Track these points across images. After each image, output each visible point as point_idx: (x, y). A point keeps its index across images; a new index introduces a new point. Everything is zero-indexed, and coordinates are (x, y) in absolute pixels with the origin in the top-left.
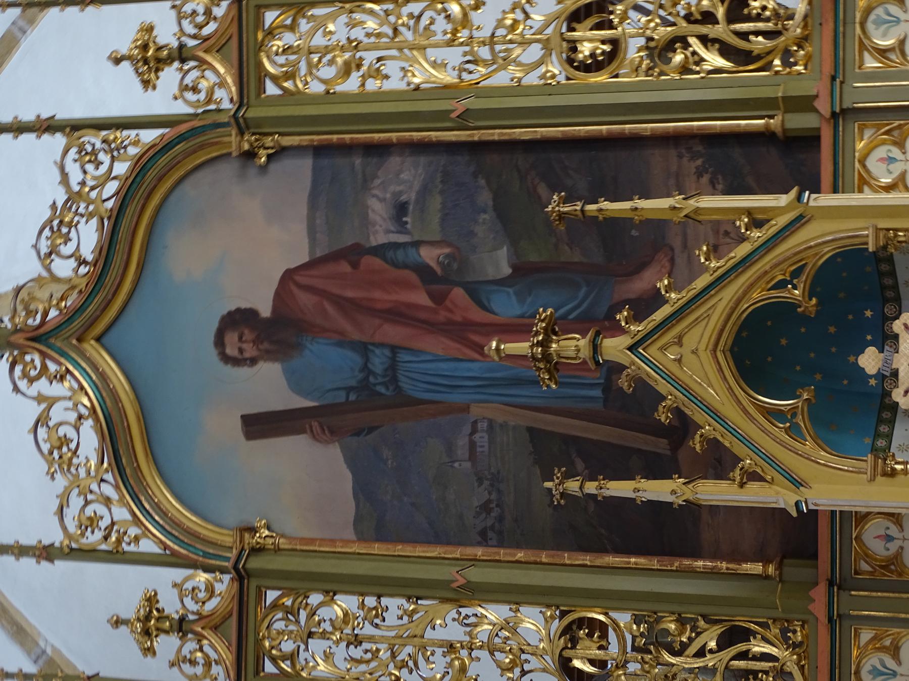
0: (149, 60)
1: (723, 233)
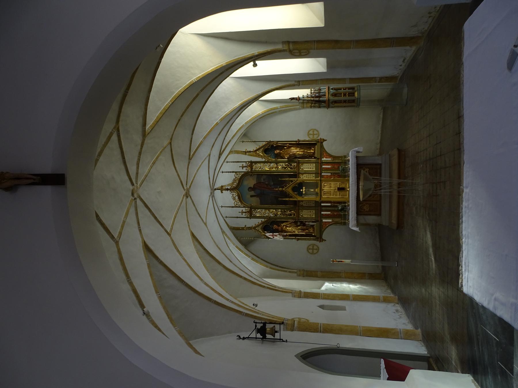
0: (243, 167)
1: (292, 181)
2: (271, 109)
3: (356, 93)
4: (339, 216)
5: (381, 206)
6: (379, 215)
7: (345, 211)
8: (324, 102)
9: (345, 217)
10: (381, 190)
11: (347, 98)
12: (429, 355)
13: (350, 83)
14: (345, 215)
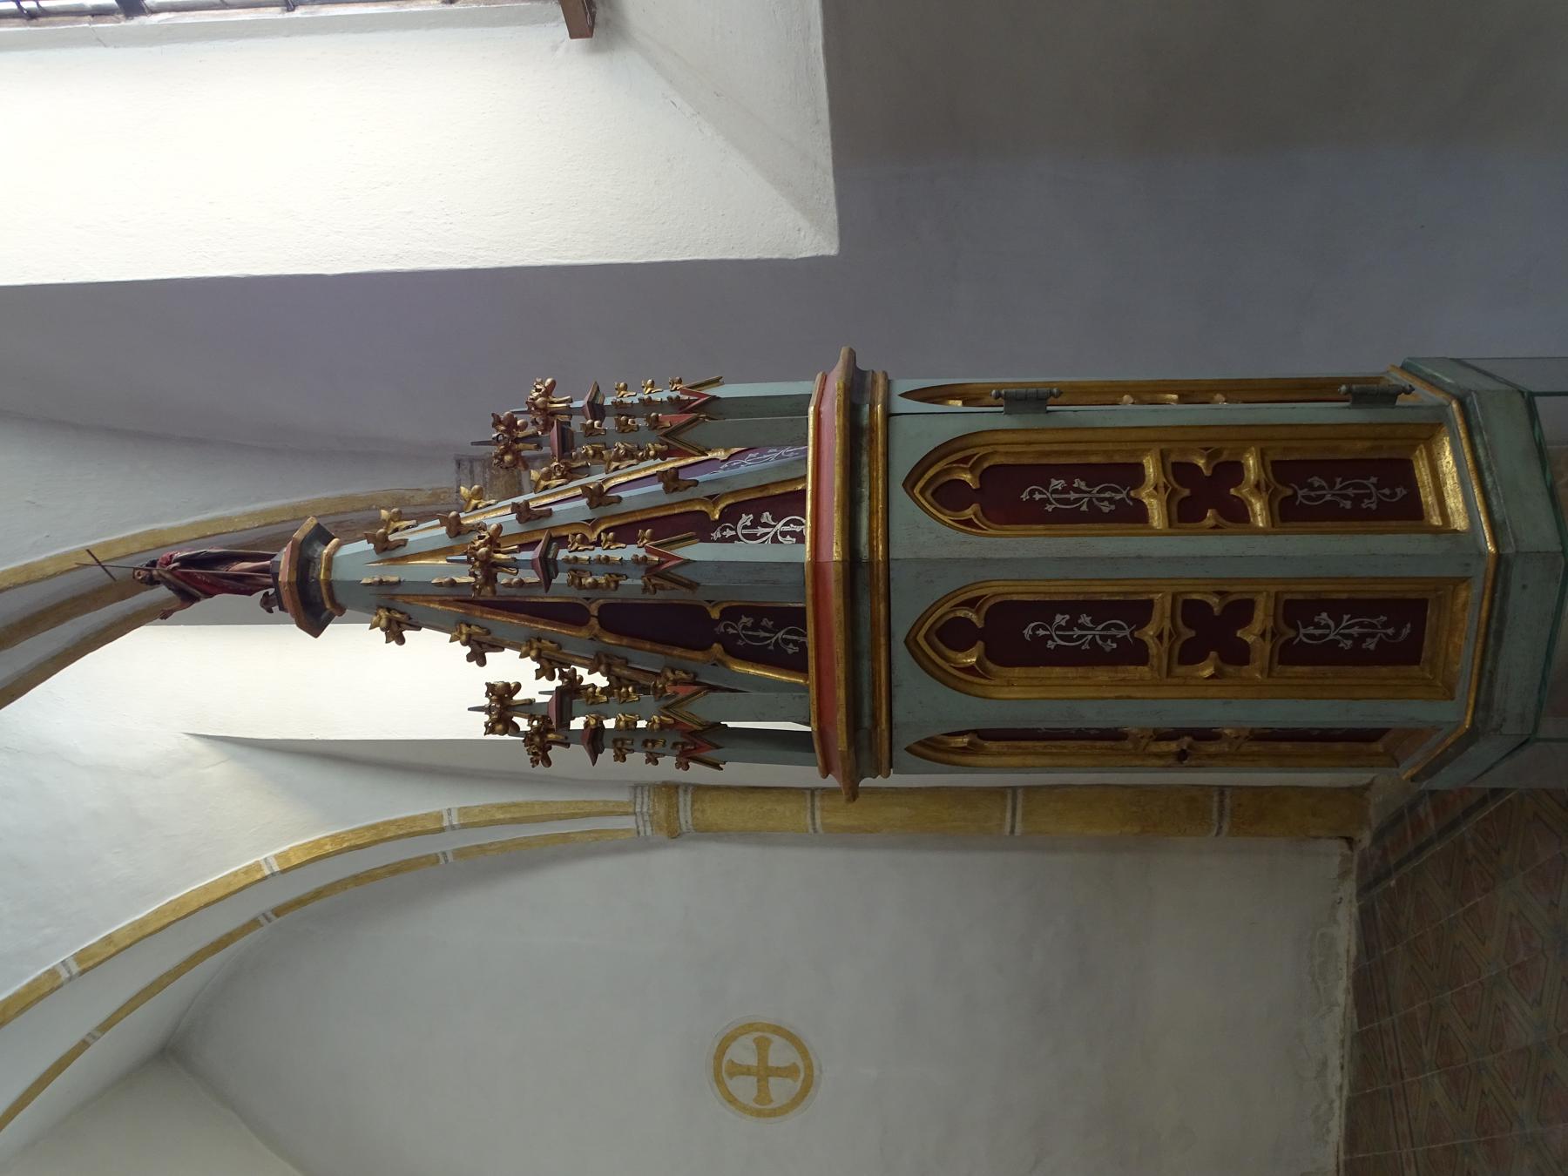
2: (379, 836)
8: (762, 629)
11: (1259, 550)
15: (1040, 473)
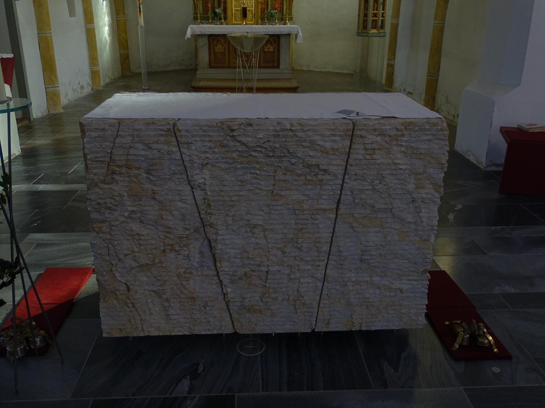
3: (375, 31)
4: (206, 11)
5: (223, 67)
6: (211, 67)
7: (213, 19)
9: (205, 19)
10: (244, 67)
11: (370, 18)
12: (32, 119)
13: (392, 25)
14: (208, 19)
15: (377, 4)
